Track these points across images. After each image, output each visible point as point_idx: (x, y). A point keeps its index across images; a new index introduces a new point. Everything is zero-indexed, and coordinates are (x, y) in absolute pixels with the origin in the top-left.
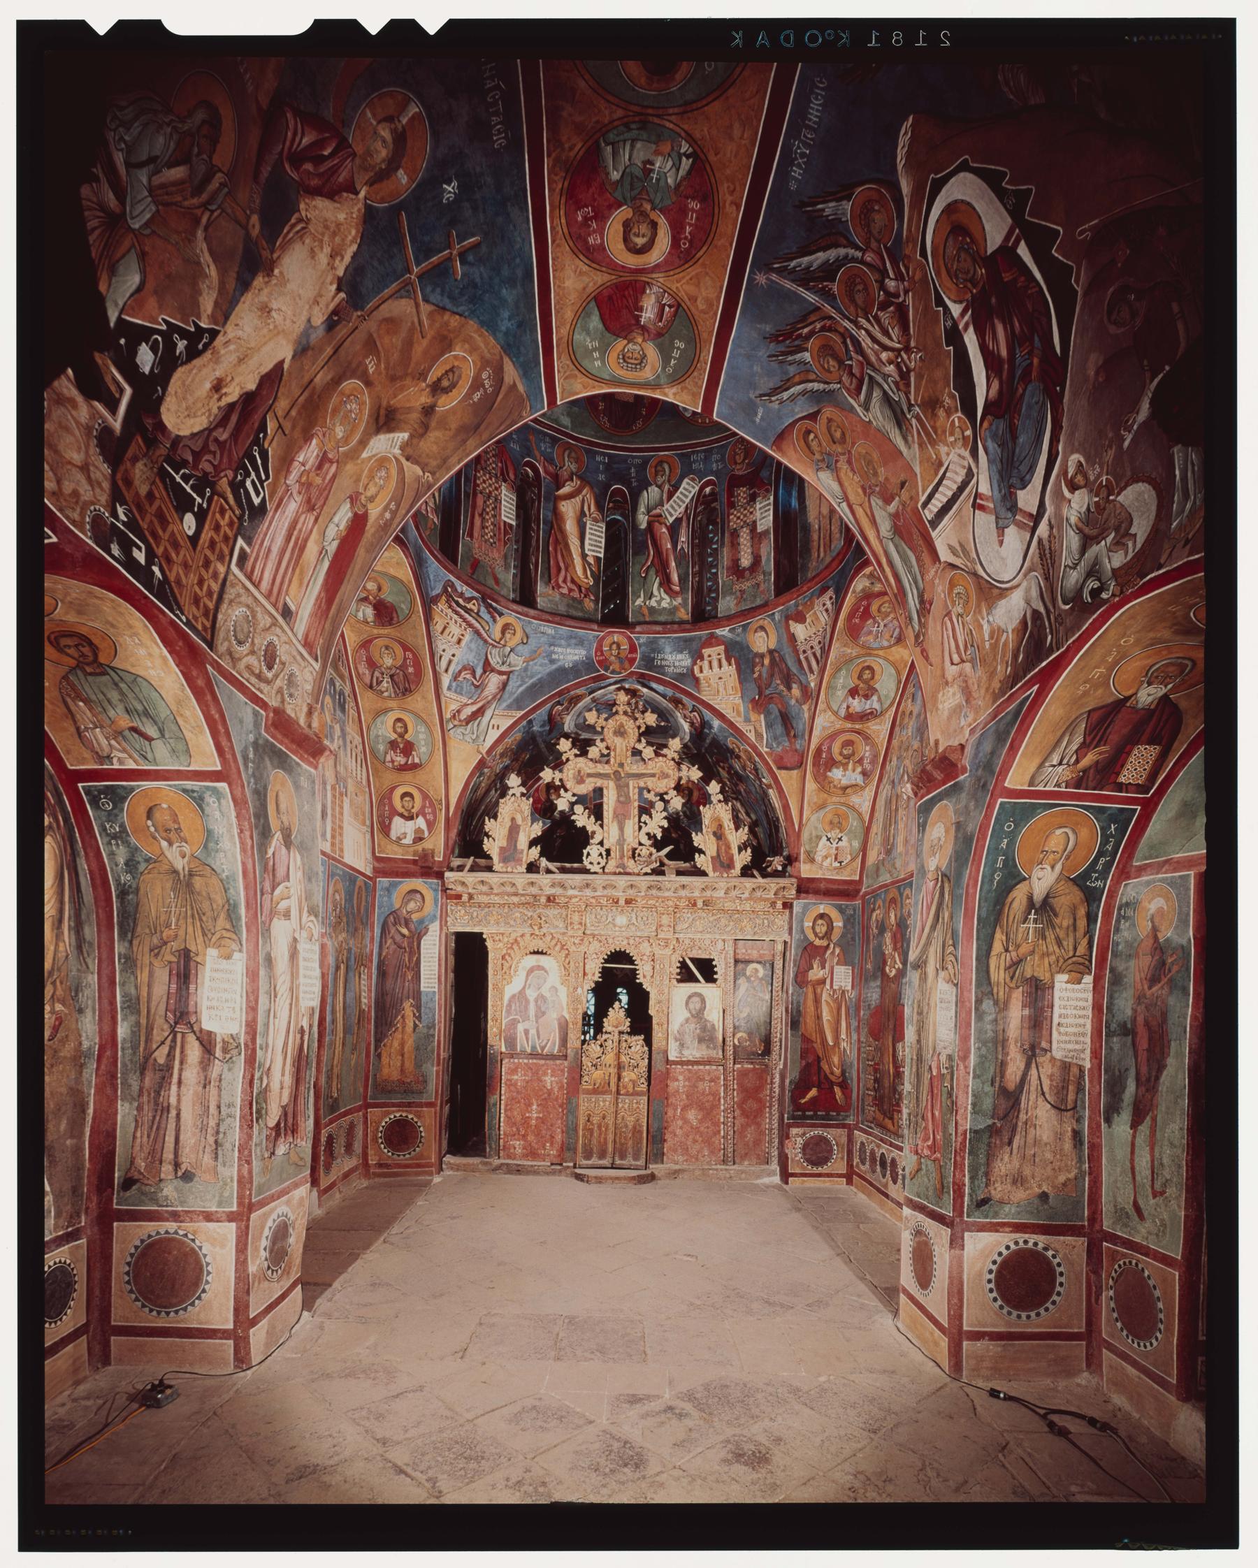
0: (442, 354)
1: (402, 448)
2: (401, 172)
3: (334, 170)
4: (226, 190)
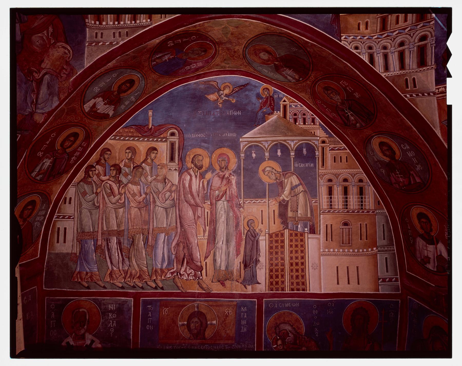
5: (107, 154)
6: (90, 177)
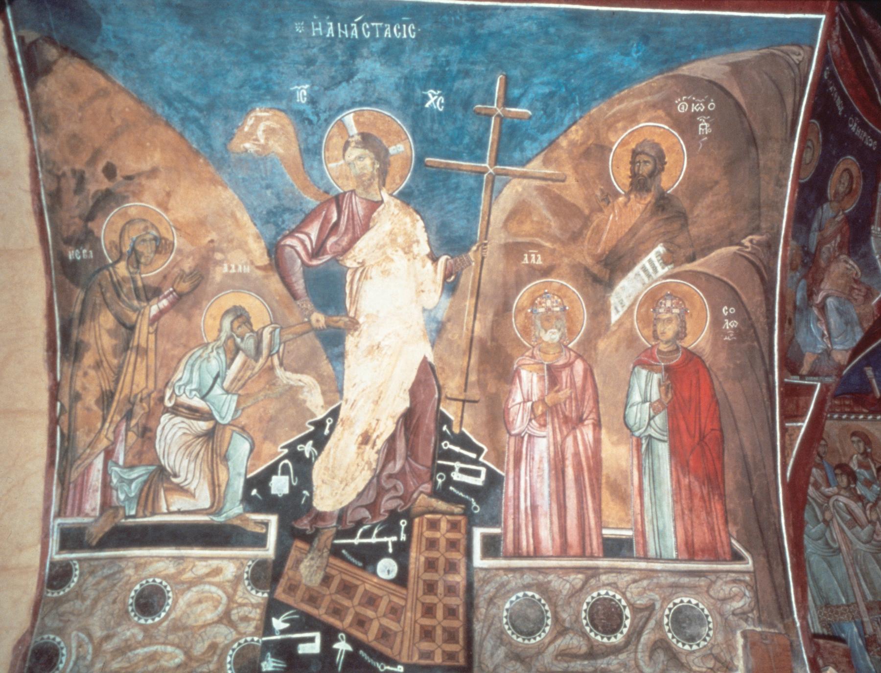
1: (665, 263)
2: (392, 150)
3: (352, 217)
4: (278, 331)
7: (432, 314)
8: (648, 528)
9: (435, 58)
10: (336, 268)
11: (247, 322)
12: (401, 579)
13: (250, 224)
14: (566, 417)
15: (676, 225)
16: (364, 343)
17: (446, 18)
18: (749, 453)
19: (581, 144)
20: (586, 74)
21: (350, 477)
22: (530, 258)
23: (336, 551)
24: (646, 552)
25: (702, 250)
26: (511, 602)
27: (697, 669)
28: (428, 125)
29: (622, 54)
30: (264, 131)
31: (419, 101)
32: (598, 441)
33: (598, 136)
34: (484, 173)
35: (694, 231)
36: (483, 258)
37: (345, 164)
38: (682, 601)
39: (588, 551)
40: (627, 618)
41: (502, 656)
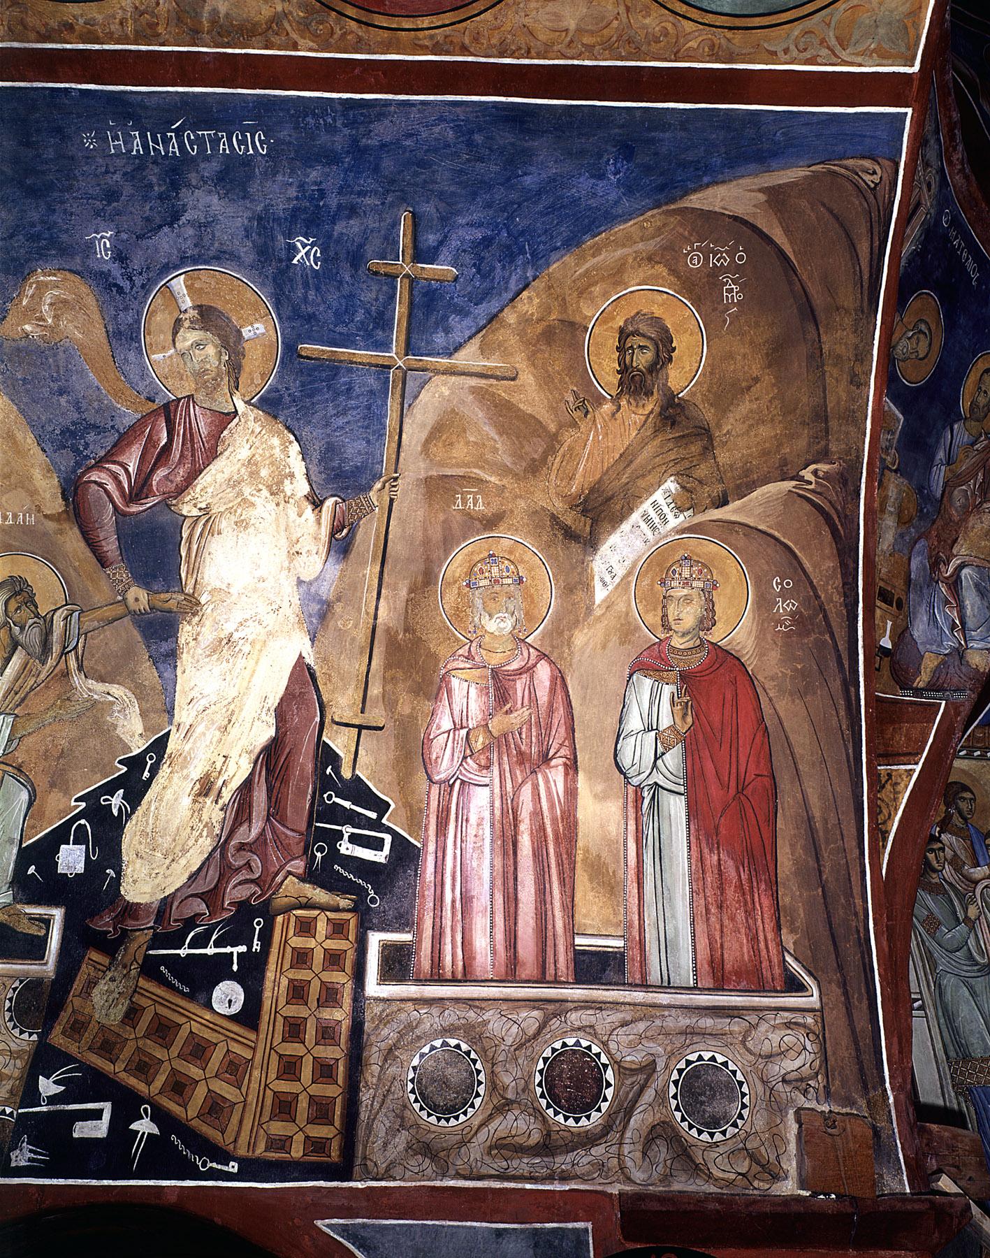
0: (576, 346)
2: (246, 332)
5: (965, 799)
6: (935, 871)
7: (313, 590)
8: (650, 935)
9: (301, 186)
10: (164, 518)
11: (31, 601)
12: (249, 1016)
13: (36, 450)
14: (520, 753)
15: (695, 448)
16: (208, 634)
17: (310, 120)
18: (817, 813)
19: (539, 320)
20: (540, 207)
21: (178, 848)
22: (464, 501)
23: (150, 968)
24: (644, 976)
25: (738, 487)
26: (422, 1056)
27: (721, 1175)
28: (300, 293)
29: (592, 176)
30: (51, 304)
31: (283, 255)
32: (571, 793)
33: (564, 305)
34: (389, 367)
35: (723, 457)
36: (392, 501)
37: (178, 355)
38: (700, 1058)
39: (551, 971)
40: (608, 1085)
41: (401, 1148)
